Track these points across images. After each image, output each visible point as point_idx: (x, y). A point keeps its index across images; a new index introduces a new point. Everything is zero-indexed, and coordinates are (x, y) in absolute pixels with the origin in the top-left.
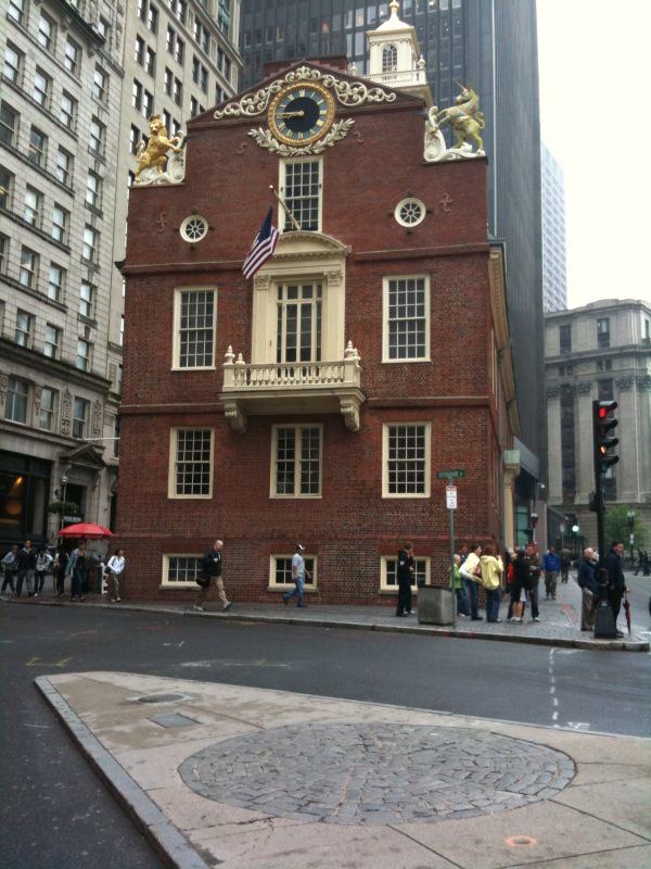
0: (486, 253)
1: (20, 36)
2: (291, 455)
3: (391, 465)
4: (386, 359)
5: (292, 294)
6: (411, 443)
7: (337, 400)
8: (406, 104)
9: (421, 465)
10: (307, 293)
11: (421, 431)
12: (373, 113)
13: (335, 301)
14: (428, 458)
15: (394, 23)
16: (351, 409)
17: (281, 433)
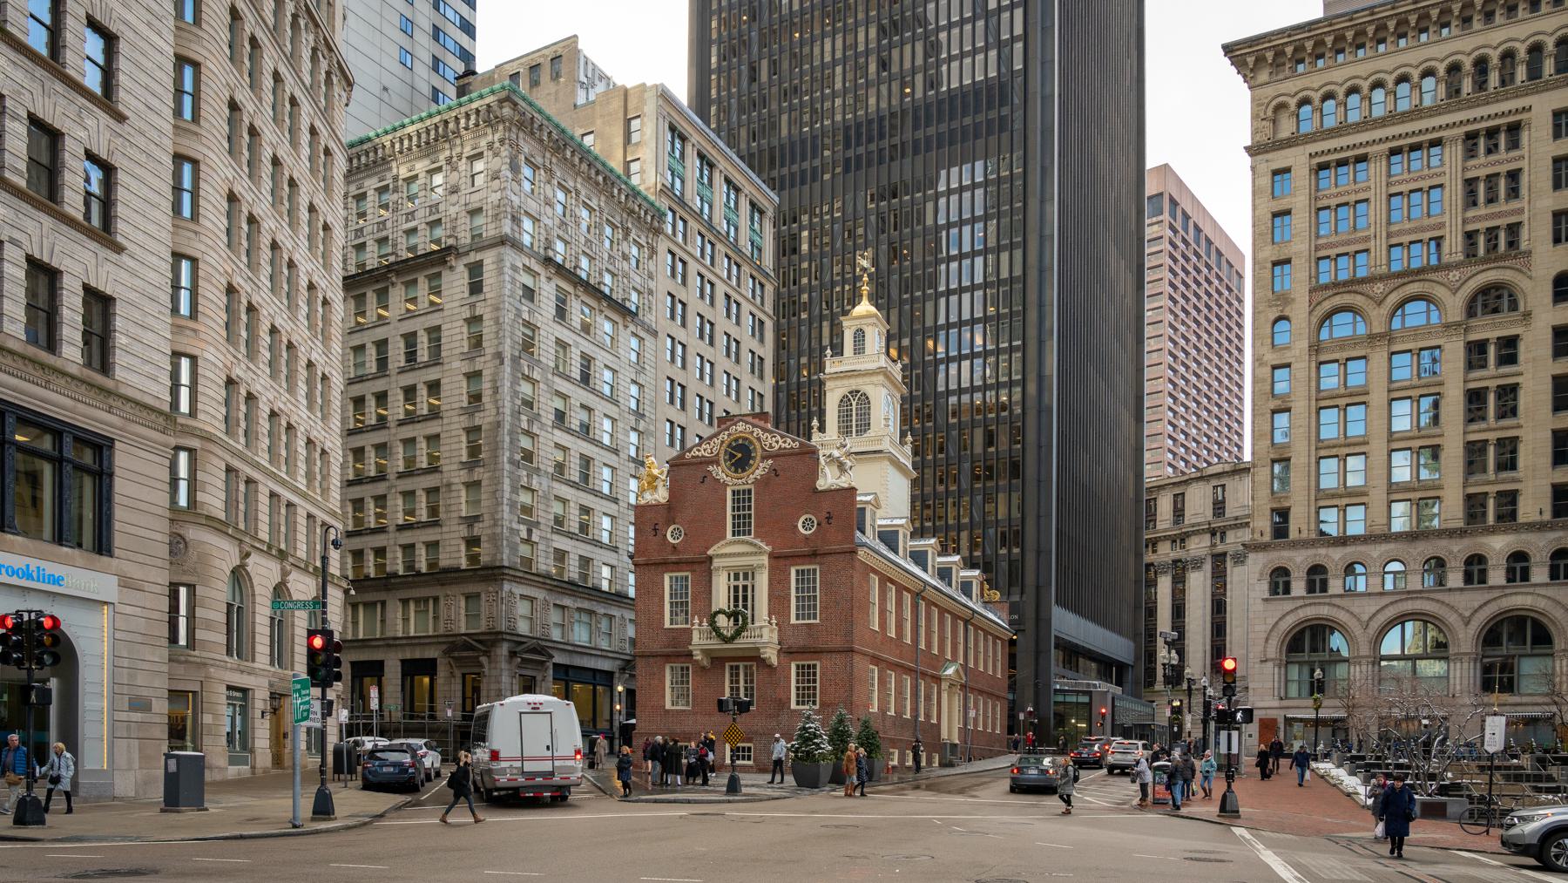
0: (853, 552)
1: (566, 332)
2: (738, 682)
3: (798, 688)
4: (793, 621)
5: (737, 577)
6: (809, 674)
7: (758, 649)
8: (805, 449)
9: (815, 688)
10: (746, 577)
11: (815, 666)
12: (783, 455)
13: (762, 581)
14: (818, 685)
15: (865, 307)
16: (771, 655)
17: (731, 667)
